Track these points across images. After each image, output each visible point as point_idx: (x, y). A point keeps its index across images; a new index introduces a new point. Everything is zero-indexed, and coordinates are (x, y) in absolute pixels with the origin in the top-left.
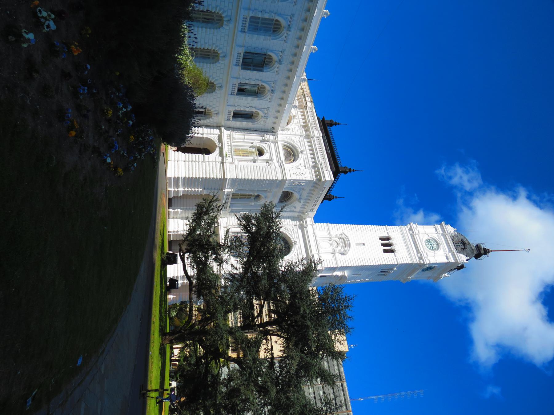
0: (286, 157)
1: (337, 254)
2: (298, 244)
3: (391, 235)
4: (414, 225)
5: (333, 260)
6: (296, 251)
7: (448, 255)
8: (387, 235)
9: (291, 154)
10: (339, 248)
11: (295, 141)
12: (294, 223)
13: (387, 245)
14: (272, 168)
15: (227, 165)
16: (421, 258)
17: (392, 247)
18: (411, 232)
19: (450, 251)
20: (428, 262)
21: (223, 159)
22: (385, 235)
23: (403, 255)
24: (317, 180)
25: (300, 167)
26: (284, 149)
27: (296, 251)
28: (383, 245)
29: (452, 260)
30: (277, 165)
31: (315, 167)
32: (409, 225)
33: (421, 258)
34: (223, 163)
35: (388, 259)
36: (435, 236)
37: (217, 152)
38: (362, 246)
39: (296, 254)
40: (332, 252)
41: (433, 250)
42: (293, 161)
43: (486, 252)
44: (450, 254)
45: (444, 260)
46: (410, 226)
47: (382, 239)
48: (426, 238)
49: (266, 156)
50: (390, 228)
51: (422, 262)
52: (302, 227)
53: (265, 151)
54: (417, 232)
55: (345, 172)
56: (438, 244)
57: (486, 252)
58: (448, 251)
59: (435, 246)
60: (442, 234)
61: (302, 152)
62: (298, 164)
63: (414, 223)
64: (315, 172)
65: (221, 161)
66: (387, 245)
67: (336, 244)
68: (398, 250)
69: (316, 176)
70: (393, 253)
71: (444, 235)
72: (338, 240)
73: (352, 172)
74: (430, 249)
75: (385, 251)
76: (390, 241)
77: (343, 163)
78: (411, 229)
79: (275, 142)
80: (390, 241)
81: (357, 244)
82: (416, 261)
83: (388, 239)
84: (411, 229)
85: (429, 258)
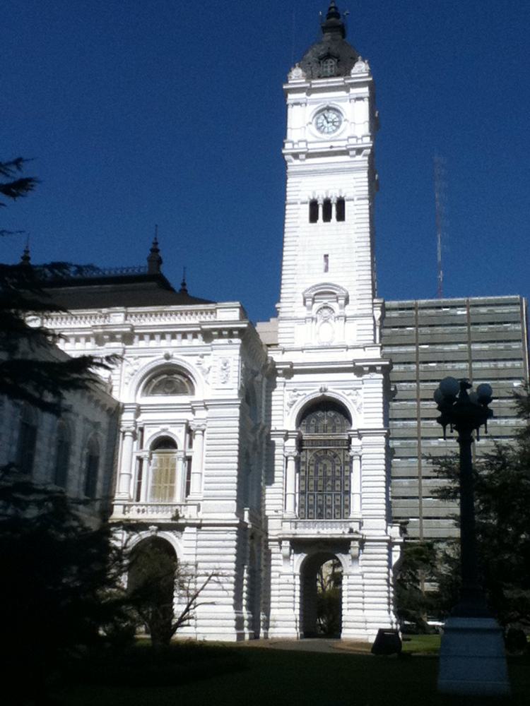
0: (175, 392)
1: (348, 314)
2: (326, 385)
3: (307, 196)
4: (288, 146)
5: (359, 322)
6: (340, 392)
7: (355, 96)
8: (307, 207)
9: (168, 378)
10: (335, 306)
11: (136, 367)
12: (279, 387)
13: (327, 210)
14: (209, 424)
15: (203, 516)
16: (359, 151)
17: (334, 201)
18: (302, 156)
19: (346, 88)
20: (367, 140)
21: (192, 525)
22: (306, 210)
23: (351, 183)
24: (239, 336)
25: (206, 366)
26: (154, 392)
27: (340, 392)
28: (327, 218)
29: (365, 91)
30: (201, 414)
31: (208, 335)
32: (287, 157)
33: (359, 151)
34: (199, 526)
35: (358, 212)
36: (311, 109)
37: (168, 536)
38: (329, 258)
39: (347, 392)
40: (344, 321)
41: (340, 122)
42: (185, 376)
43: (334, 14)
44: (353, 91)
45: (364, 106)
46: (288, 154)
47: (313, 218)
48: (313, 128)
49: (179, 435)
50: (290, 196)
51: (368, 151)
52: (289, 373)
53: (163, 434)
54: (303, 145)
55: (160, 261)
56: (328, 109)
57: (334, 14)
58: (343, 93)
59: (332, 116)
60: (308, 94)
61: (167, 357)
62: (199, 371)
63: (283, 146)
64: (220, 336)
65: (194, 530)
66: (327, 210)
67: (326, 311)
68: (340, 191)
69: (231, 335)
70: (347, 204)
71: (310, 91)
72: (316, 306)
73: (159, 247)
74: (338, 127)
75: (341, 217)
76: (320, 202)
77: (138, 262)
78: (296, 156)
79: (138, 411)
80: (320, 202)
81: (326, 269)
82: (362, 161)
83: (314, 205)
84: (296, 156)
85: (359, 136)
